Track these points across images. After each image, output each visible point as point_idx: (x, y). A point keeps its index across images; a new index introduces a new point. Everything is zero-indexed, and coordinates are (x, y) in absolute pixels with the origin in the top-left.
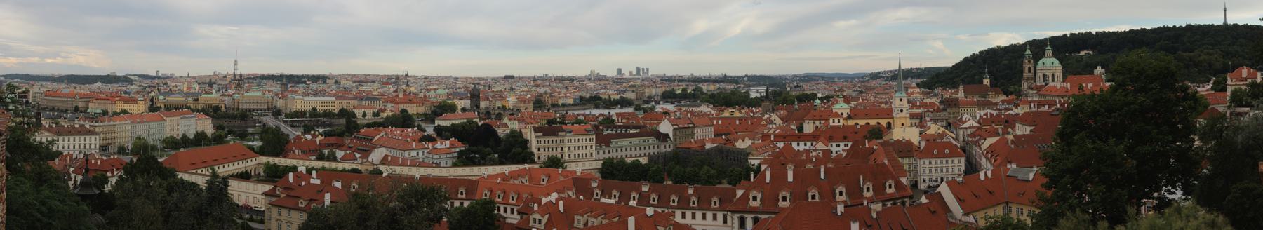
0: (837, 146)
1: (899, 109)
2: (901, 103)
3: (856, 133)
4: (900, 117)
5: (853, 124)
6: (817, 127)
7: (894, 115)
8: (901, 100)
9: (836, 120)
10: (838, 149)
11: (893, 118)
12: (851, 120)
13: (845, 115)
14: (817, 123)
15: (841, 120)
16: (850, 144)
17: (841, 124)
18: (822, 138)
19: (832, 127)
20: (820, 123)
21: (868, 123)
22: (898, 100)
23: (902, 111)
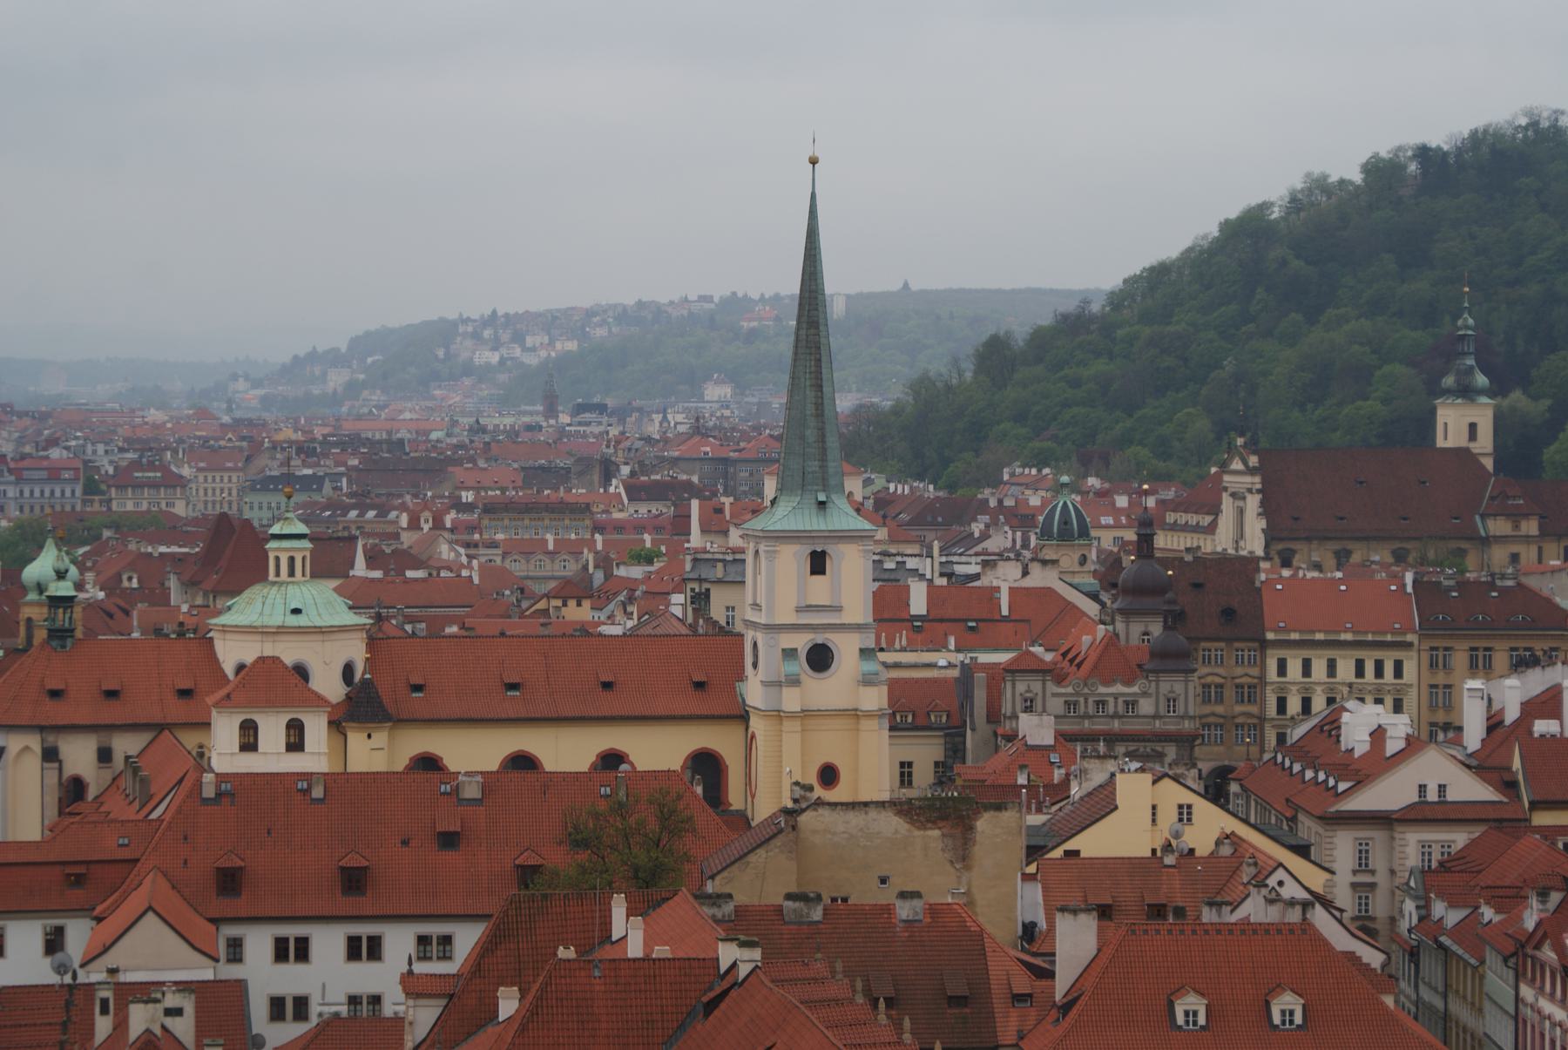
0: (281, 952)
1: (802, 642)
2: (819, 588)
3: (449, 840)
4: (806, 714)
5: (400, 764)
6: (74, 789)
7: (753, 692)
8: (818, 563)
9: (272, 730)
10: (291, 979)
11: (742, 717)
12: (381, 738)
13: (330, 685)
14: (79, 755)
15: (316, 729)
16: (467, 938)
17: (317, 757)
18: (149, 887)
19: (237, 789)
20: (105, 755)
21: (522, 762)
22: (793, 559)
23: (820, 658)
